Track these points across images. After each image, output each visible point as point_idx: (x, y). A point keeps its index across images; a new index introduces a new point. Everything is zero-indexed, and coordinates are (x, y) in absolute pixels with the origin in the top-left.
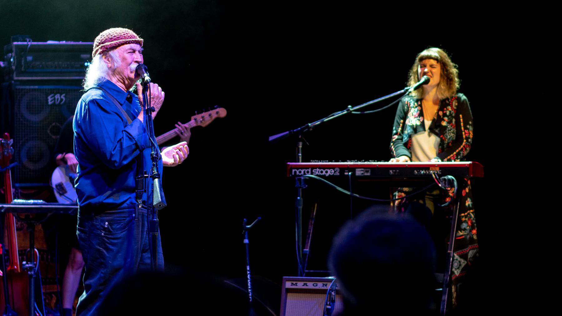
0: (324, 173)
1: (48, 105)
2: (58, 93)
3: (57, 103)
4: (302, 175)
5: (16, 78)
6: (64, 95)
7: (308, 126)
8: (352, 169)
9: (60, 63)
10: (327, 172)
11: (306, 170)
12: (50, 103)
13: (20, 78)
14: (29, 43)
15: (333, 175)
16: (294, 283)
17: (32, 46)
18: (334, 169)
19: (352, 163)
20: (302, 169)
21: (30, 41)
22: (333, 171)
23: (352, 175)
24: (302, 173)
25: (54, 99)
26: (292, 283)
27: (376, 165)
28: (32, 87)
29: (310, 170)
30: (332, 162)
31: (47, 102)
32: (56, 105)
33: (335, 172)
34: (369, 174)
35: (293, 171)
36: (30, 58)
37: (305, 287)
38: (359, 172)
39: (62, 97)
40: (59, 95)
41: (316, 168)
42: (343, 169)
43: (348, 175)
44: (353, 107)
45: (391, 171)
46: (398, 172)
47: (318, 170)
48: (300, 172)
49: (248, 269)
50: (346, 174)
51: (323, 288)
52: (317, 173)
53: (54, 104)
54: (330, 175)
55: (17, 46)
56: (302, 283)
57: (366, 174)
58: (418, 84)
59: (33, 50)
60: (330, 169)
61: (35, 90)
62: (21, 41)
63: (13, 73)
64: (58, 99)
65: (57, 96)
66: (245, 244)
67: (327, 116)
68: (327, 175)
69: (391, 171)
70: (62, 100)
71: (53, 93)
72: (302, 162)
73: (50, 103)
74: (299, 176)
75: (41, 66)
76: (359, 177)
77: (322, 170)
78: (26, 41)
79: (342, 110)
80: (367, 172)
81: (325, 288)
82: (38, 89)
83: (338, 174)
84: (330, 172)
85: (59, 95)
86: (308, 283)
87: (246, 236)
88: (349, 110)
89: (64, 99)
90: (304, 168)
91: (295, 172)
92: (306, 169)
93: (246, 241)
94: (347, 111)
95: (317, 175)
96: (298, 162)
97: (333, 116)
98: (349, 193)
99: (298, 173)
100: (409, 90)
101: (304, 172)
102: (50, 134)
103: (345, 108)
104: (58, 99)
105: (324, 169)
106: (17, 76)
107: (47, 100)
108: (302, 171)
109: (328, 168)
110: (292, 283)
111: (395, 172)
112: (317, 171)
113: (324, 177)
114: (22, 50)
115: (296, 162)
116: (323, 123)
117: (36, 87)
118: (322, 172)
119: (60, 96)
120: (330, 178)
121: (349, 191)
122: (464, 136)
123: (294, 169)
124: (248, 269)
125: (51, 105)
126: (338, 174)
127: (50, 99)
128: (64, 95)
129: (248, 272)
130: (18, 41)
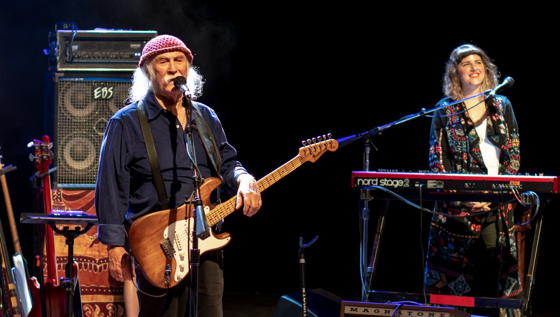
0: (392, 184)
1: (95, 100)
2: (106, 86)
3: (104, 97)
4: (368, 185)
5: (60, 69)
6: (112, 88)
7: (377, 129)
8: (424, 180)
10: (395, 183)
11: (373, 180)
12: (96, 97)
15: (402, 186)
16: (354, 308)
17: (77, 34)
18: (403, 180)
19: (424, 174)
20: (368, 178)
21: (75, 29)
22: (403, 183)
23: (422, 187)
24: (369, 183)
25: (101, 93)
26: (352, 309)
27: (451, 177)
28: (77, 79)
29: (377, 180)
30: (401, 171)
31: (93, 96)
32: (103, 100)
33: (404, 183)
34: (442, 187)
35: (359, 180)
36: (75, 47)
37: (366, 313)
38: (431, 184)
39: (109, 91)
40: (106, 88)
41: (384, 179)
42: (413, 180)
43: (419, 187)
44: (427, 110)
45: (466, 184)
46: (475, 186)
47: (386, 180)
48: (366, 182)
49: (304, 291)
50: (417, 185)
51: (385, 315)
52: (385, 183)
53: (100, 99)
54: (398, 186)
55: (61, 33)
56: (363, 309)
57: (438, 187)
58: (500, 86)
59: (79, 39)
60: (399, 179)
61: (80, 82)
64: (105, 93)
65: (104, 90)
66: (301, 264)
67: (398, 119)
68: (396, 186)
69: (466, 184)
70: (109, 94)
71: (100, 85)
72: (369, 170)
73: (96, 97)
74: (364, 185)
75: (87, 56)
76: (431, 190)
77: (390, 180)
79: (415, 113)
80: (440, 184)
81: (387, 315)
82: (83, 82)
83: (407, 185)
84: (399, 183)
85: (106, 88)
86: (369, 309)
87: (302, 255)
88: (423, 113)
89: (111, 92)
90: (370, 178)
91: (361, 182)
92: (373, 178)
93: (303, 261)
94: (420, 114)
95: (385, 186)
96: (365, 171)
97: (405, 119)
98: (419, 207)
99: (363, 183)
100: (490, 93)
101: (371, 182)
102: (96, 130)
103: (419, 110)
104: (105, 93)
105: (393, 180)
106: (60, 68)
107: (93, 93)
108: (369, 181)
109: (396, 179)
110: (352, 309)
111: (471, 186)
112: (385, 182)
113: (392, 188)
114: (67, 38)
115: (363, 170)
116: (394, 127)
117: (82, 79)
118: (390, 183)
119: (108, 90)
120: (399, 190)
121: (419, 205)
123: (360, 178)
124: (304, 291)
125: (97, 99)
126: (407, 185)
127: (96, 92)
128: (112, 88)
129: (304, 295)
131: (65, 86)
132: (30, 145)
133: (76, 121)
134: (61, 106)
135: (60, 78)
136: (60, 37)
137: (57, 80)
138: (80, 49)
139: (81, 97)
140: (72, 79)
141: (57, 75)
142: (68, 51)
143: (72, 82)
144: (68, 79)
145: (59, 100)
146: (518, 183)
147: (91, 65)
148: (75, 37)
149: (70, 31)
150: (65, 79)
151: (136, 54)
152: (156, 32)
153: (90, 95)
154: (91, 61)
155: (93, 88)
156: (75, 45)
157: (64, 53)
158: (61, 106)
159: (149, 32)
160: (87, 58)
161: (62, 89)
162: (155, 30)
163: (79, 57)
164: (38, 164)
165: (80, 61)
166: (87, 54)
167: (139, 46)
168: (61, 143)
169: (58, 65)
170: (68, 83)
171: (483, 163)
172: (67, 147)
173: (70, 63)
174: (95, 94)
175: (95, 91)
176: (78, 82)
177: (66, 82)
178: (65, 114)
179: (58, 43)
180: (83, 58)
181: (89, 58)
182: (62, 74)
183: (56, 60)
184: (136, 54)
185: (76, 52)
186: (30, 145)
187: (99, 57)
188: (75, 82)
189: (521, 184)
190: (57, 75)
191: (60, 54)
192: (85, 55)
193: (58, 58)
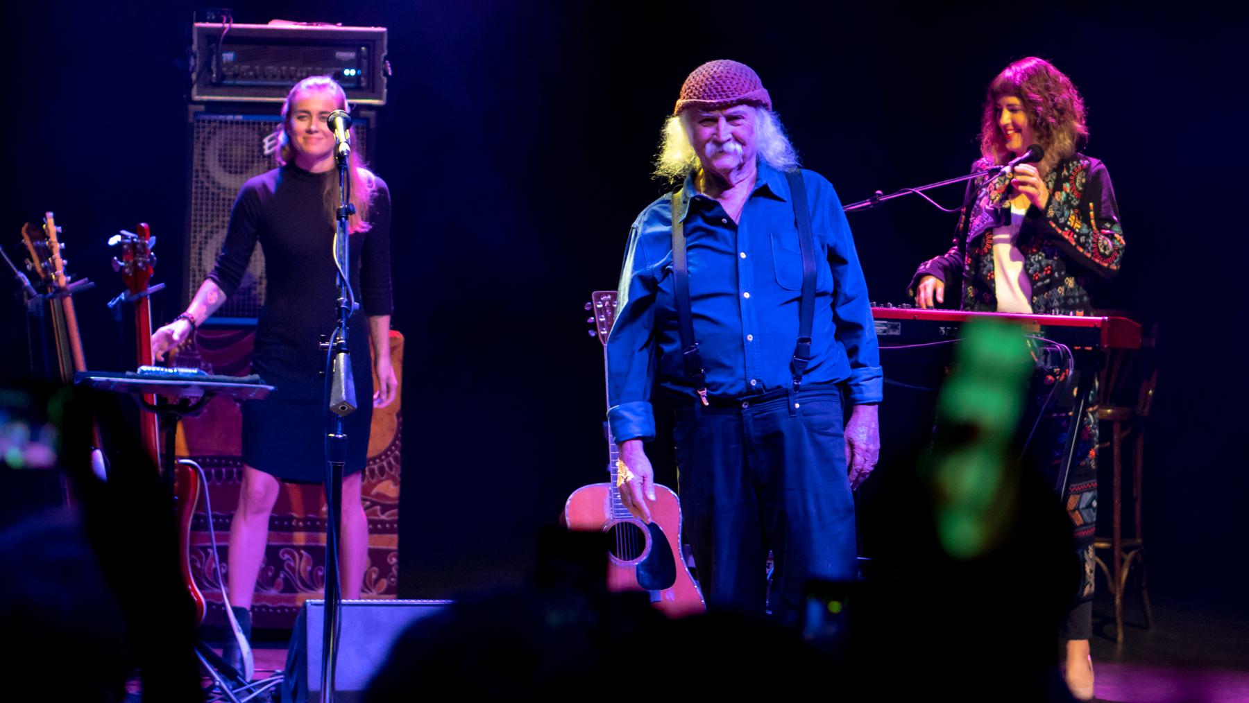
1: (264, 157)
5: (197, 98)
9: (293, 68)
12: (267, 152)
13: (205, 98)
14: (227, 25)
17: (231, 29)
21: (228, 22)
28: (230, 117)
31: (262, 150)
34: (897, 333)
36: (228, 56)
55: (200, 29)
57: (891, 333)
59: (234, 40)
61: (237, 123)
62: (211, 21)
63: (191, 87)
73: (267, 152)
78: (220, 21)
80: (894, 328)
106: (199, 93)
107: (261, 145)
117: (240, 117)
122: (1089, 255)
127: (267, 142)
130: (204, 21)
131: (207, 130)
132: (114, 240)
133: (227, 196)
134: (199, 168)
135: (196, 114)
136: (199, 35)
137: (191, 119)
138: (238, 60)
139: (239, 151)
140: (222, 117)
141: (192, 108)
142: (214, 62)
143: (221, 122)
144: (214, 117)
145: (195, 157)
146: (1037, 328)
147: (258, 91)
148: (226, 36)
149: (219, 25)
150: (207, 117)
151: (347, 72)
152: (384, 29)
153: (256, 149)
154: (259, 83)
155: (263, 135)
156: (227, 51)
157: (206, 66)
158: (199, 168)
159: (373, 29)
160: (250, 78)
161: (202, 135)
162: (382, 26)
163: (235, 76)
164: (126, 275)
165: (238, 82)
166: (252, 69)
167: (352, 55)
168: (198, 239)
169: (194, 90)
170: (213, 125)
171: (994, 289)
172: (209, 247)
173: (218, 85)
174: (266, 147)
175: (266, 140)
176: (232, 122)
177: (209, 122)
178: (206, 184)
179: (195, 47)
180: (244, 78)
181: (256, 77)
182: (202, 108)
183: (191, 79)
184: (347, 72)
185: (229, 65)
186: (114, 240)
187: (274, 76)
188: (226, 122)
189: (1042, 329)
190: (192, 108)
191: (197, 69)
192: (248, 71)
193: (194, 76)
